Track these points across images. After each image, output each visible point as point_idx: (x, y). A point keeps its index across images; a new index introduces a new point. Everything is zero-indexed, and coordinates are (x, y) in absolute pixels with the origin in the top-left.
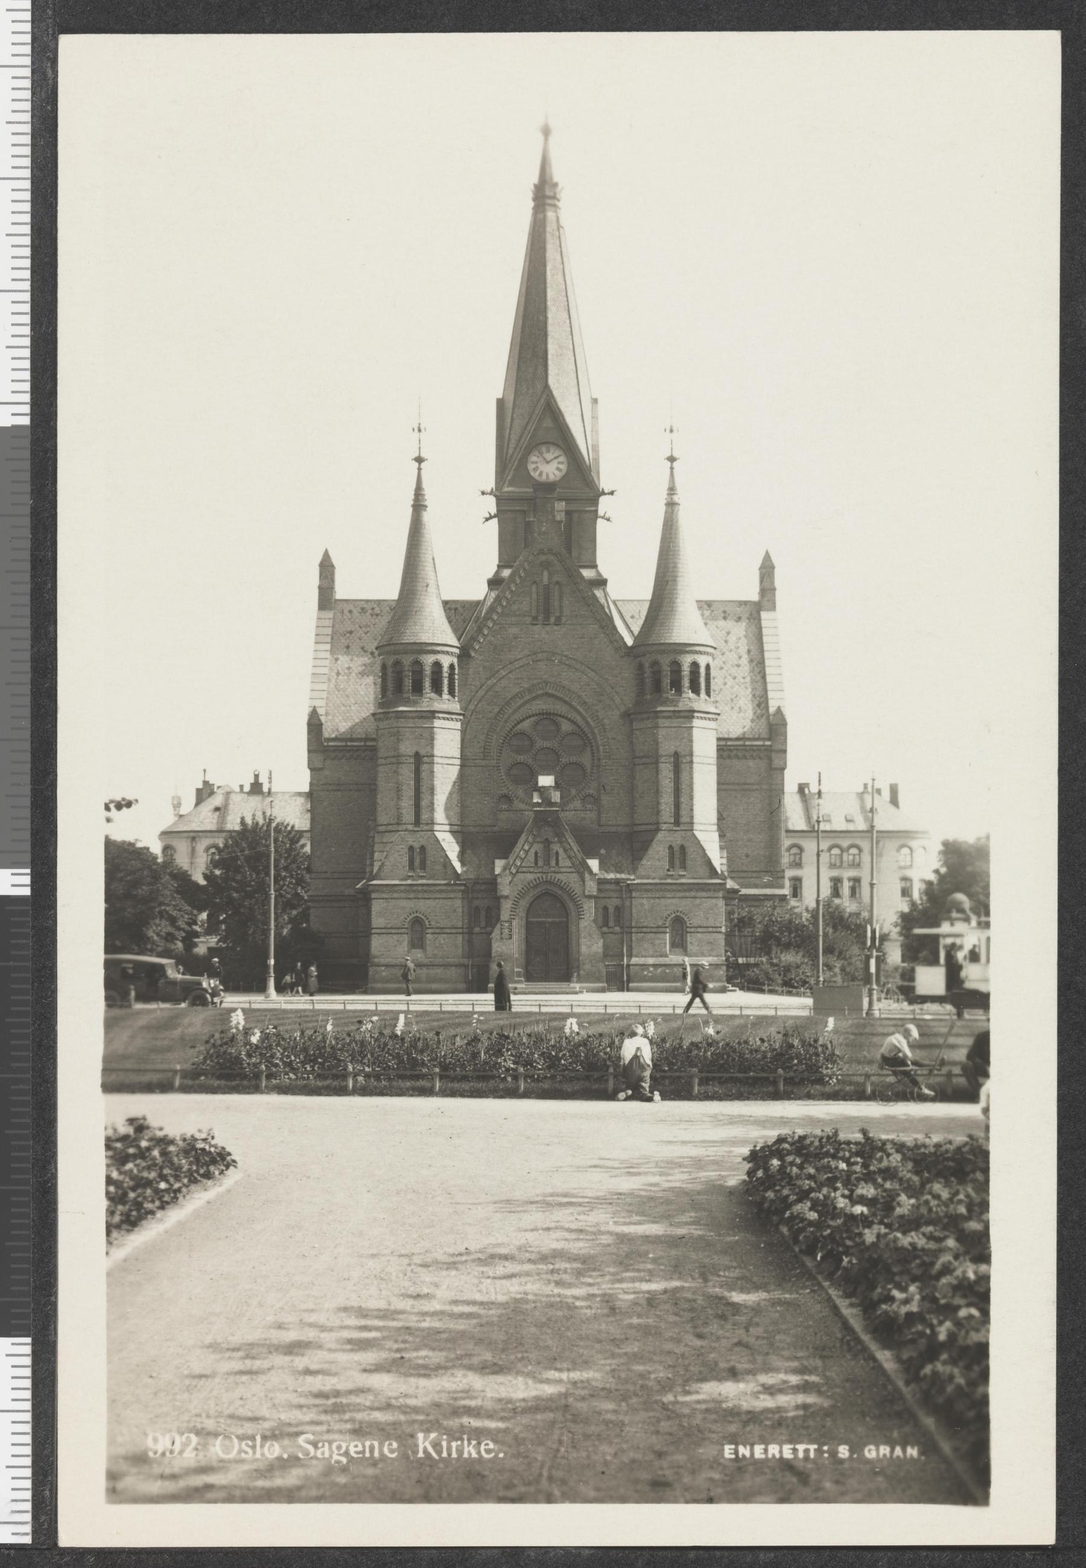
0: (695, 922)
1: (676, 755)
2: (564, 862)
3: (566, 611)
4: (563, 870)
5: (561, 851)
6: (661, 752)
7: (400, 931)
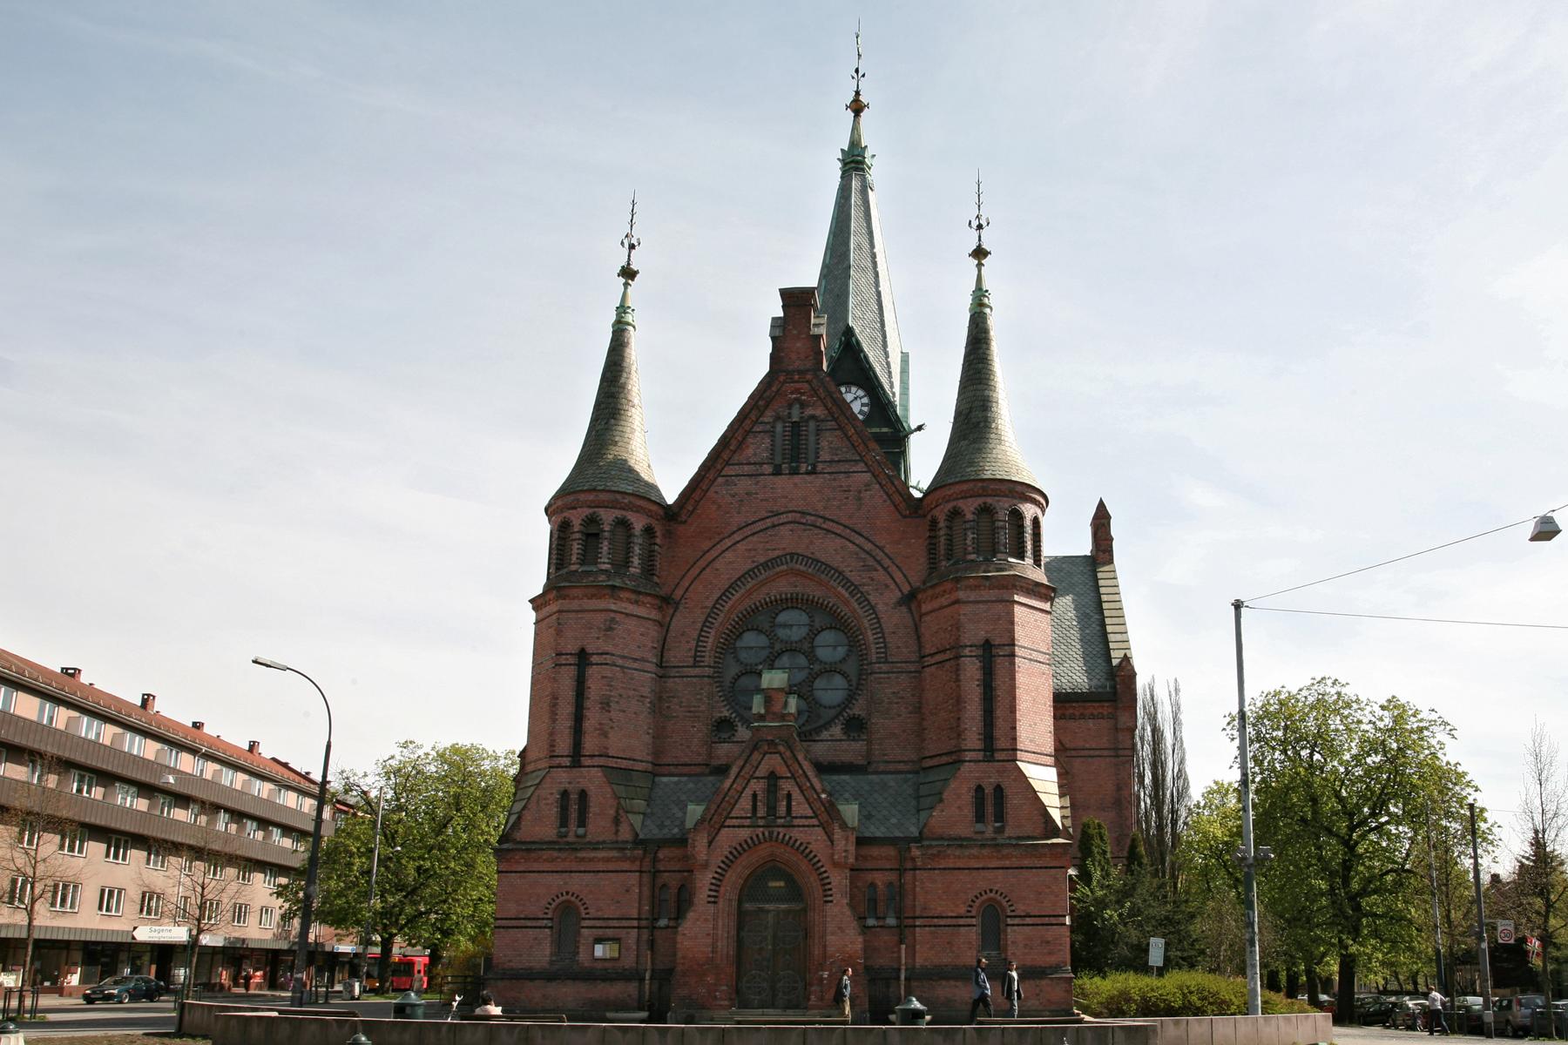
0: (1021, 909)
1: (987, 645)
2: (801, 808)
3: (825, 456)
4: (796, 822)
5: (796, 794)
7: (539, 923)
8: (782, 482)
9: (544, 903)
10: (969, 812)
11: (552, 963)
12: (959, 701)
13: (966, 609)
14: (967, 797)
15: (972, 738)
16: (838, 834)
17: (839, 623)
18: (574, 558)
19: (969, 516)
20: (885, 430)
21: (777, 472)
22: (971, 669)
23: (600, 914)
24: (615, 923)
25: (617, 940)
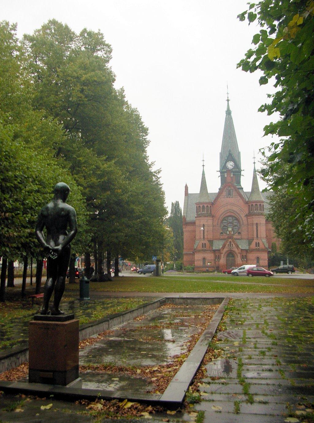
1: (257, 224)
3: (234, 195)
5: (233, 244)
8: (228, 199)
10: (255, 246)
13: (254, 219)
14: (255, 244)
15: (255, 236)
16: (239, 249)
17: (237, 219)
19: (254, 205)
20: (237, 170)
21: (227, 197)
22: (255, 227)
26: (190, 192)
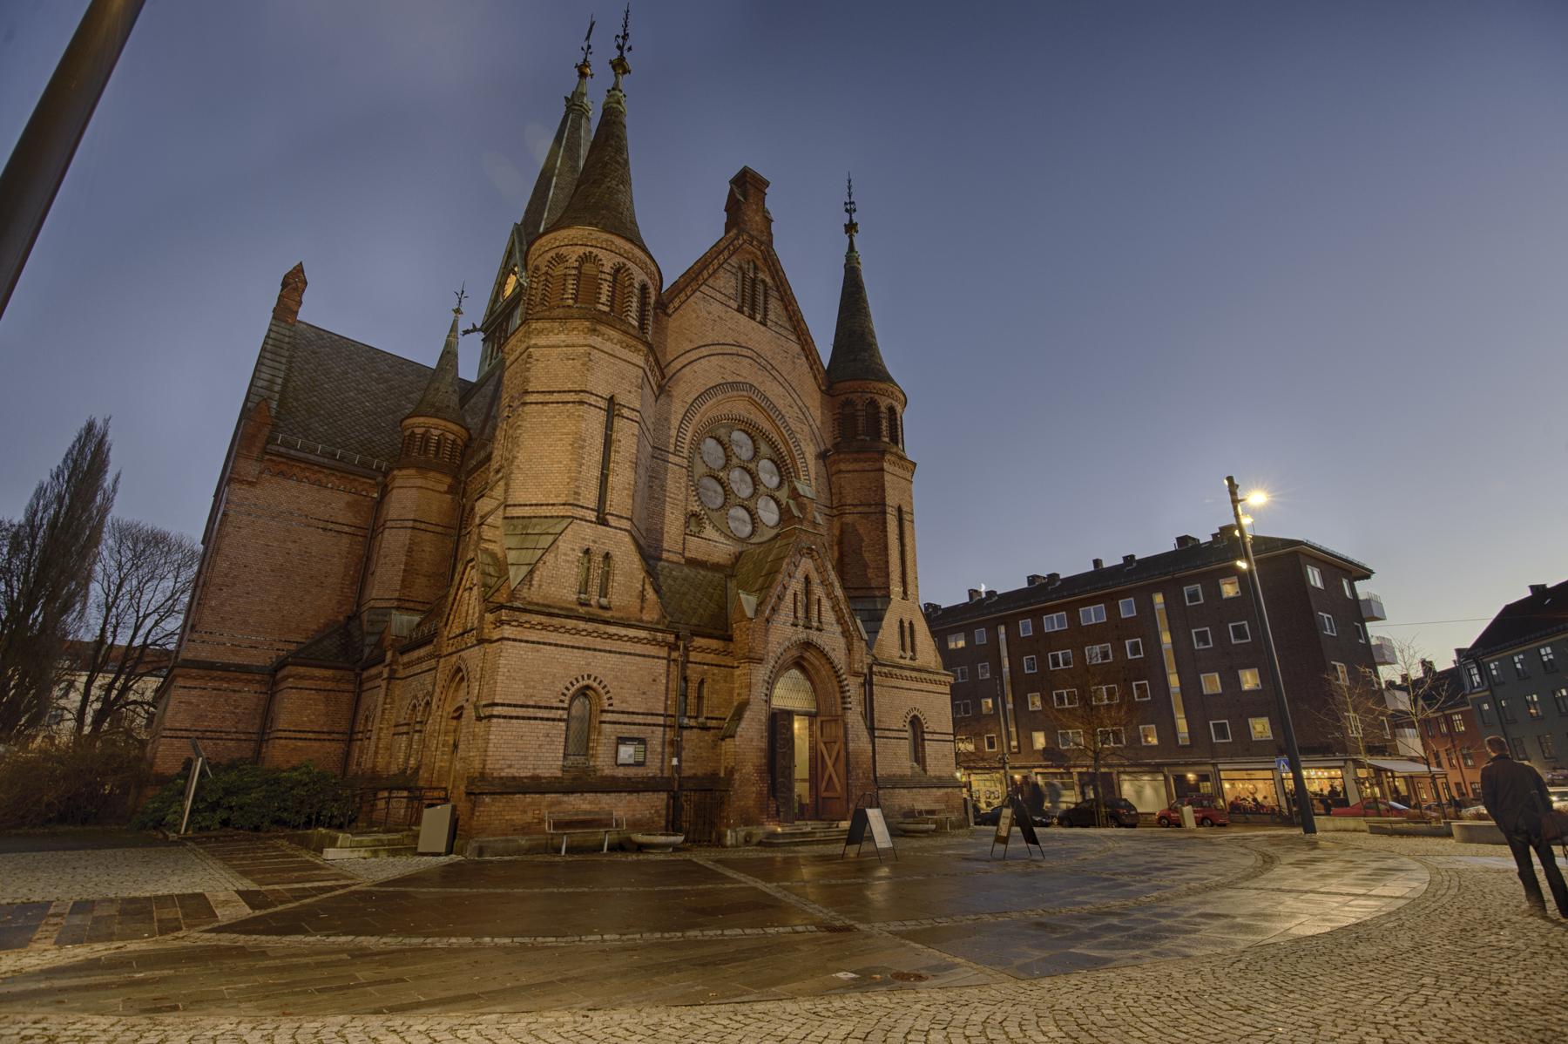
3: (771, 316)
5: (825, 601)
6: (888, 501)
7: (552, 714)
8: (743, 319)
9: (560, 687)
11: (564, 769)
12: (886, 547)
18: (604, 299)
23: (624, 707)
24: (639, 719)
25: (642, 741)
26: (310, 313)
